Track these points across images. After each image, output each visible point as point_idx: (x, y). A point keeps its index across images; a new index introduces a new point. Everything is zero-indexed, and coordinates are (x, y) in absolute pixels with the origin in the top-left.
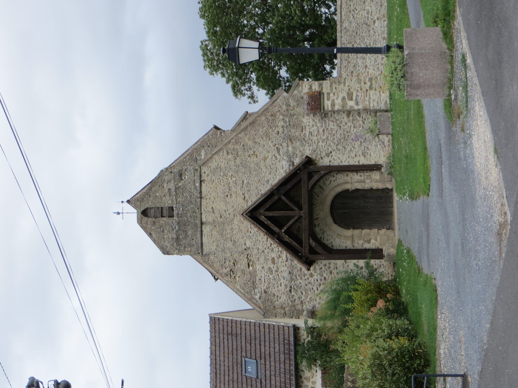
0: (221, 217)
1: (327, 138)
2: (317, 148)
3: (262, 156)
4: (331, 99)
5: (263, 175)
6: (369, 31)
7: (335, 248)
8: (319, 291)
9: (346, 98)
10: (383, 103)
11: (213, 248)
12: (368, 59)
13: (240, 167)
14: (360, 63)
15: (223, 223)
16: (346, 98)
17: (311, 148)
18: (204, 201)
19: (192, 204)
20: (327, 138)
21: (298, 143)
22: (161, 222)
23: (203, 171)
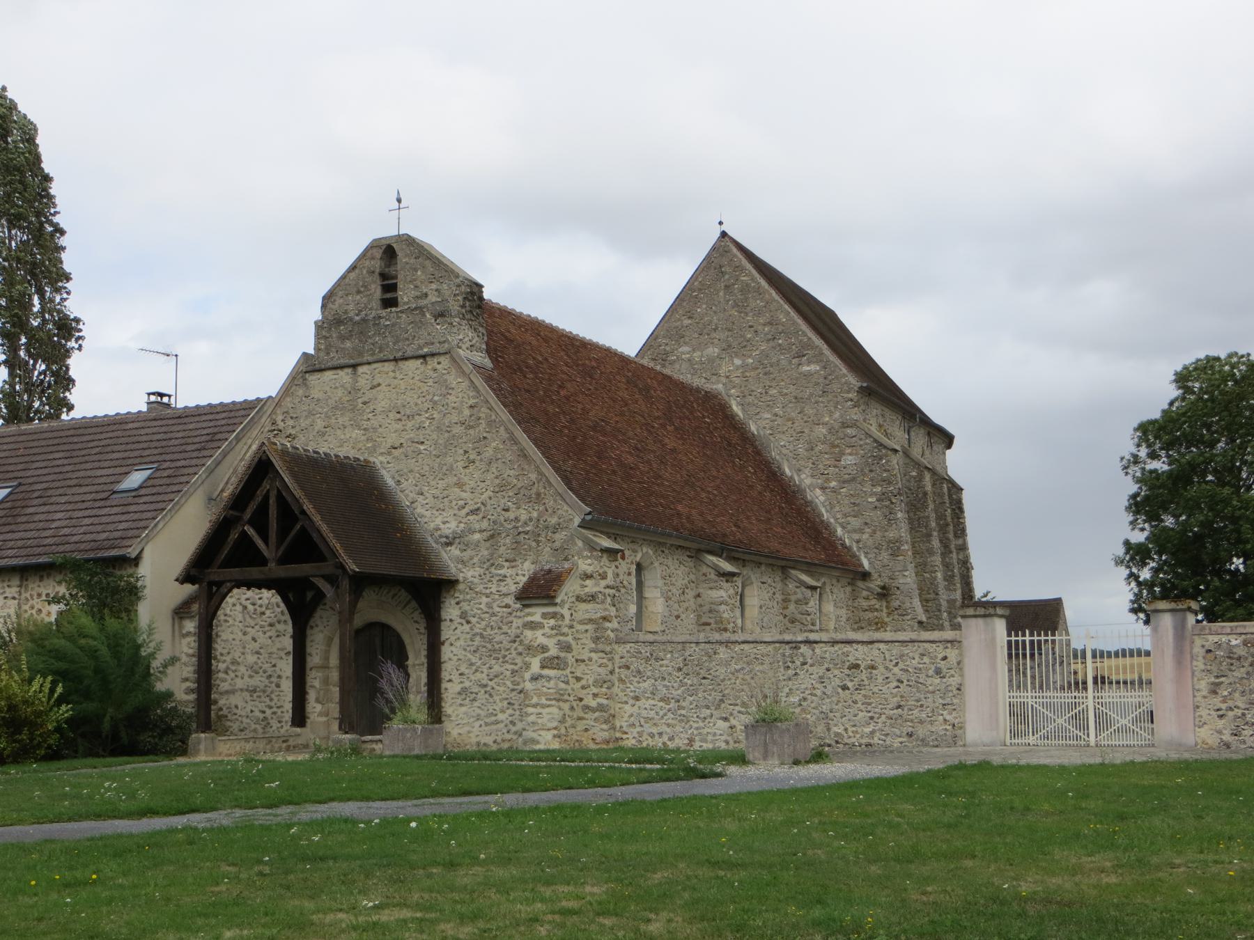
0: (365, 403)
1: (494, 614)
2: (477, 593)
3: (466, 479)
4: (545, 621)
5: (433, 483)
6: (708, 707)
7: (309, 632)
8: (244, 602)
9: (546, 655)
10: (534, 735)
11: (316, 394)
12: (652, 702)
13: (446, 435)
14: (645, 685)
15: (353, 410)
16: (546, 655)
17: (476, 581)
18: (388, 367)
19: (394, 344)
20: (494, 614)
21: (486, 553)
22: (373, 286)
23: (442, 359)
